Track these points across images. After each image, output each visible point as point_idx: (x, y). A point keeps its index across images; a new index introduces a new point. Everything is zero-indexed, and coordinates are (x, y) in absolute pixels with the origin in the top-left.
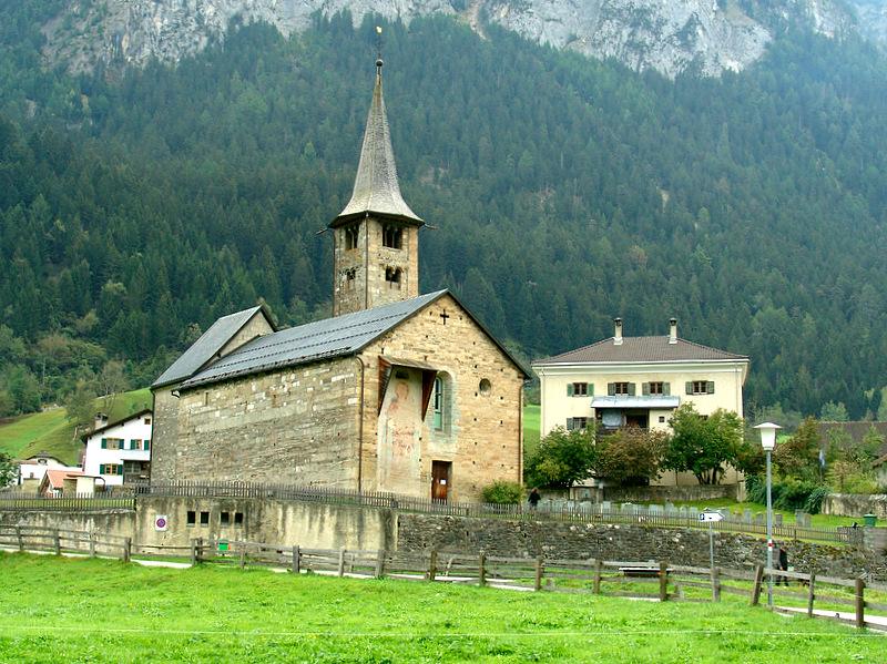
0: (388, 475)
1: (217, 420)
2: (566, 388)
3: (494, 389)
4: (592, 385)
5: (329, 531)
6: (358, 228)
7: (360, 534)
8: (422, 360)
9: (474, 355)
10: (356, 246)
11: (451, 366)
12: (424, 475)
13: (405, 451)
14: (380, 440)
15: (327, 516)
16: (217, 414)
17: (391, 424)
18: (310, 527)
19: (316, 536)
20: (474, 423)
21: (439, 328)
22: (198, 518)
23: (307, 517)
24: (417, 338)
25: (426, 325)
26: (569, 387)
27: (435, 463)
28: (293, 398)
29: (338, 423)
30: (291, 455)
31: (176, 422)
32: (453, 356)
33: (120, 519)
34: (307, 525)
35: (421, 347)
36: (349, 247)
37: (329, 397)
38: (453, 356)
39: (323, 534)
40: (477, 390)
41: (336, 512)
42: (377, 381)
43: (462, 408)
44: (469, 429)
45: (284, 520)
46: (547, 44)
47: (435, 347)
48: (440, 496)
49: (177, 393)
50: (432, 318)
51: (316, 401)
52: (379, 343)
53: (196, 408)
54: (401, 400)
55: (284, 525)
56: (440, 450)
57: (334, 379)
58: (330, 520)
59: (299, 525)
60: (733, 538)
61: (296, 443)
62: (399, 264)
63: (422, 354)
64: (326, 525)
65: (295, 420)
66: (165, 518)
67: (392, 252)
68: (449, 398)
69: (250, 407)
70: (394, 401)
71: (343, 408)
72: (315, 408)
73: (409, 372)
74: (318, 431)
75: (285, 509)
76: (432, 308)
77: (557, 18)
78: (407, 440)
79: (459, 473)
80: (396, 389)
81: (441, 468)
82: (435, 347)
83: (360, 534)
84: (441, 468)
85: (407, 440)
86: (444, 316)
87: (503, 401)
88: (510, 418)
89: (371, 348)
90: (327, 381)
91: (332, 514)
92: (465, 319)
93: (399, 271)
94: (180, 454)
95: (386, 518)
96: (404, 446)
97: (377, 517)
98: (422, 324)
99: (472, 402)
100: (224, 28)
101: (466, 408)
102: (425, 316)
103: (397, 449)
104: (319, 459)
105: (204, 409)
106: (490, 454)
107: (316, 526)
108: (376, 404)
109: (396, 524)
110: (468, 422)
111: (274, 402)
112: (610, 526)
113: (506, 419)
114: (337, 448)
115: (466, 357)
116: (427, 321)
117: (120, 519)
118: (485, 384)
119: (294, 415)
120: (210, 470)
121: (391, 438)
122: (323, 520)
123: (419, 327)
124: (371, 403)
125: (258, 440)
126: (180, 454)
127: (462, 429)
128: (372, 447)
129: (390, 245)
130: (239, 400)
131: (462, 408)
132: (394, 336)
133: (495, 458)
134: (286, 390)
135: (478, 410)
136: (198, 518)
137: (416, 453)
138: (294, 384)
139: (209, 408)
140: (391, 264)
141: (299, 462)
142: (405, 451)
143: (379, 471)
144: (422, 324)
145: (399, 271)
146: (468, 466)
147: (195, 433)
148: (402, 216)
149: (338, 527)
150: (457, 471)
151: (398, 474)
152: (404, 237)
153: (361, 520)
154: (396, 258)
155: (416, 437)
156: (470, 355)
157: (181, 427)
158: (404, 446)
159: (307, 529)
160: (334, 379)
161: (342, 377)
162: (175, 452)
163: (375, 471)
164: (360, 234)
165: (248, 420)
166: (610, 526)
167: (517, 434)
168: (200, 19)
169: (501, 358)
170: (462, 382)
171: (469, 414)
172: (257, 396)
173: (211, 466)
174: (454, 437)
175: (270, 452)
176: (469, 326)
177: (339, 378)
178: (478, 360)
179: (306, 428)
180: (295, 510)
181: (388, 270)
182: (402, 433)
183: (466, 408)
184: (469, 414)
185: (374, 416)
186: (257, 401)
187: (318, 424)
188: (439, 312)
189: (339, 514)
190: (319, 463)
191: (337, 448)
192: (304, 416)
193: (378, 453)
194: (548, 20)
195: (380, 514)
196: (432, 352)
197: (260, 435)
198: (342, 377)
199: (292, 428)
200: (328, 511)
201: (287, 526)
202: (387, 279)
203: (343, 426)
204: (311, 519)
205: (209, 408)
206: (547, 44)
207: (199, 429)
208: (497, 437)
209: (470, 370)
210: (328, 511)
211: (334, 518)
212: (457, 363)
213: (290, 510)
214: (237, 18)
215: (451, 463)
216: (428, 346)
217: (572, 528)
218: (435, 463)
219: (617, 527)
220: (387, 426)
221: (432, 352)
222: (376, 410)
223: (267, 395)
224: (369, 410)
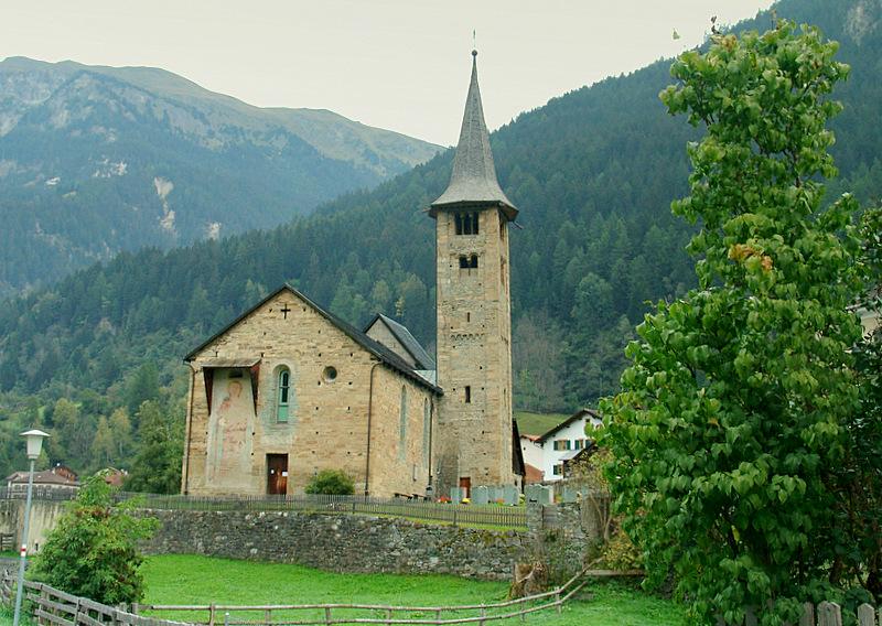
9: (318, 344)
11: (290, 358)
12: (256, 469)
13: (236, 447)
14: (210, 439)
17: (222, 422)
20: (315, 412)
23: (43, 514)
25: (264, 322)
27: (270, 456)
32: (293, 348)
38: (293, 348)
43: (302, 398)
47: (273, 343)
48: (275, 487)
50: (272, 314)
52: (214, 347)
54: (234, 399)
56: (275, 444)
60: (389, 524)
62: (473, 250)
67: (466, 239)
70: (227, 400)
73: (244, 371)
76: (272, 305)
78: (237, 436)
79: (295, 464)
80: (229, 388)
81: (277, 461)
84: (277, 461)
85: (237, 436)
86: (285, 311)
87: (351, 387)
88: (360, 402)
89: (203, 354)
92: (308, 310)
93: (475, 258)
96: (235, 442)
98: (260, 323)
99: (314, 391)
102: (264, 313)
103: (228, 445)
106: (333, 442)
108: (206, 405)
112: (280, 513)
113: (354, 404)
115: (309, 347)
121: (221, 435)
123: (256, 325)
127: (301, 419)
128: (202, 445)
131: (302, 398)
132: (229, 338)
133: (338, 446)
137: (249, 446)
140: (463, 252)
143: (208, 468)
144: (260, 323)
151: (227, 469)
152: (481, 220)
154: (469, 245)
155: (249, 433)
156: (314, 345)
158: (235, 442)
163: (203, 468)
166: (280, 513)
167: (367, 418)
169: (351, 342)
170: (305, 373)
171: (309, 404)
174: (292, 429)
176: (314, 315)
178: (322, 349)
183: (307, 398)
184: (309, 404)
185: (206, 416)
188: (280, 308)
193: (208, 450)
200: (57, 507)
209: (312, 360)
210: (57, 507)
216: (265, 343)
217: (247, 517)
218: (270, 456)
220: (217, 425)
222: (206, 410)
224: (200, 411)
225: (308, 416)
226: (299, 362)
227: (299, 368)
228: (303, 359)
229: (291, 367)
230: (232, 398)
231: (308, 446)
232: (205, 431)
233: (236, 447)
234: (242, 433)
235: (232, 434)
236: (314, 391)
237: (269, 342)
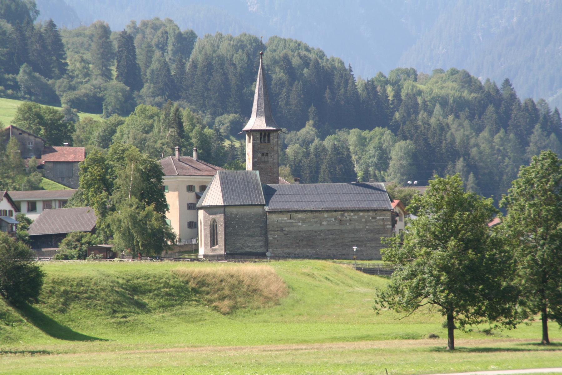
1: (300, 226)
16: (300, 224)
51: (369, 224)
53: (282, 220)
69: (325, 223)
72: (367, 227)
74: (370, 236)
105: (290, 221)
125: (330, 236)
134: (348, 218)
139: (293, 221)
147: (282, 230)
160: (378, 218)
161: (383, 217)
165: (322, 228)
172: (328, 219)
173: (297, 245)
179: (362, 234)
197: (333, 235)
198: (383, 217)
199: (353, 233)
223: (335, 219)
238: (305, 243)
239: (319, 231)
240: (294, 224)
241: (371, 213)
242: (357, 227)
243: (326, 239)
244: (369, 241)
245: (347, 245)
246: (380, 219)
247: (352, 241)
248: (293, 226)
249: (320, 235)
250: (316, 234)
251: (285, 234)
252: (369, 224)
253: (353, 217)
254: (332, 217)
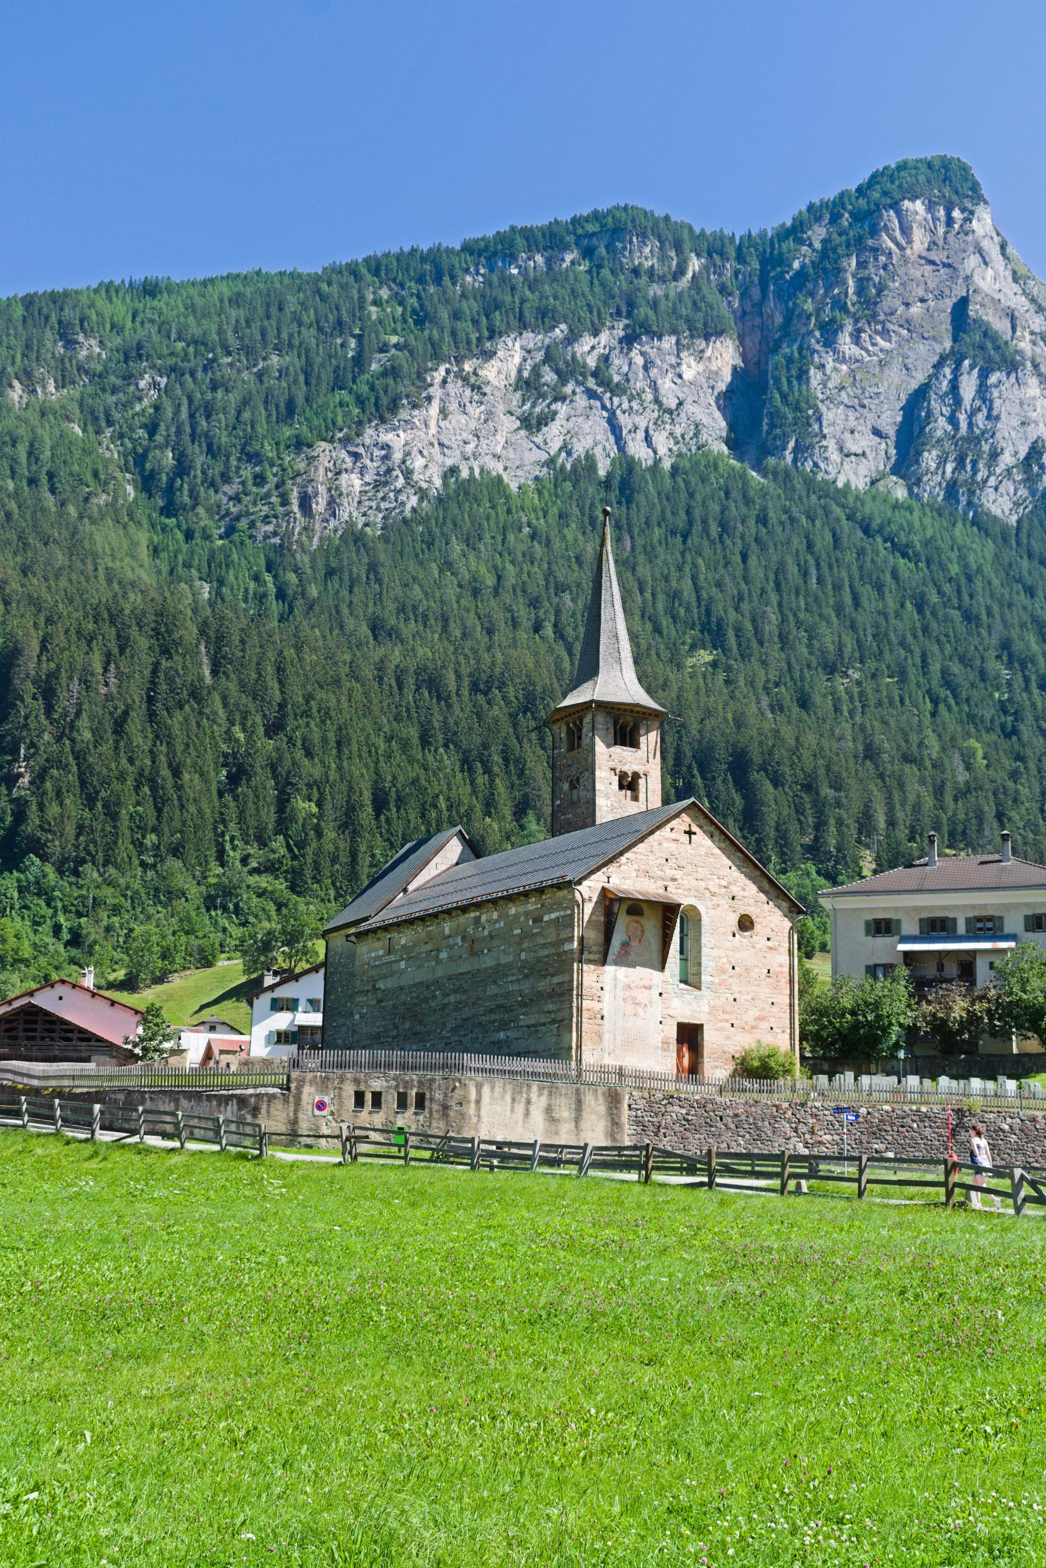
0: (618, 1042)
1: (403, 972)
2: (863, 926)
3: (758, 927)
4: (898, 921)
5: (538, 1115)
6: (581, 722)
7: (577, 1120)
8: (662, 891)
10: (579, 746)
12: (665, 1042)
14: (607, 996)
15: (534, 1096)
16: (403, 964)
18: (512, 1111)
19: (520, 1123)
21: (683, 849)
22: (368, 1098)
23: (508, 1098)
24: (654, 862)
25: (666, 845)
26: (868, 924)
28: (495, 943)
29: (552, 975)
30: (493, 1017)
31: (352, 975)
33: (269, 1101)
34: (508, 1108)
35: (660, 873)
36: (571, 748)
37: (541, 941)
38: (702, 884)
39: (531, 1120)
40: (735, 928)
41: (546, 1092)
42: (602, 919)
44: (724, 980)
45: (478, 1102)
46: (847, 485)
47: (678, 874)
49: (353, 938)
50: (673, 835)
51: (525, 945)
53: (377, 958)
55: (478, 1109)
57: (546, 918)
58: (539, 1102)
59: (498, 1109)
61: (501, 1001)
63: (661, 883)
64: (531, 1108)
65: (498, 973)
66: (326, 1099)
68: (698, 940)
69: (443, 955)
71: (559, 955)
72: (523, 956)
73: (644, 906)
74: (526, 986)
75: (479, 1087)
77: (859, 451)
78: (642, 996)
82: (678, 874)
83: (577, 1120)
86: (690, 833)
87: (770, 944)
90: (538, 920)
91: (540, 1095)
94: (357, 1017)
95: (613, 1099)
97: (601, 1100)
98: (660, 844)
99: (728, 944)
100: (438, 482)
101: (722, 953)
102: (665, 832)
103: (629, 1008)
104: (529, 1023)
105: (387, 959)
106: (754, 1013)
107: (520, 1108)
108: (601, 949)
109: (626, 1107)
110: (724, 972)
111: (472, 947)
112: (914, 1108)
114: (551, 1007)
115: (720, 886)
116: (667, 839)
117: (269, 1101)
118: (746, 924)
119: (498, 964)
120: (395, 1037)
121: (620, 993)
122: (528, 1102)
123: (656, 847)
124: (594, 948)
125: (452, 998)
126: (357, 1017)
127: (716, 980)
129: (624, 744)
130: (429, 947)
131: (715, 952)
133: (760, 1019)
134: (486, 933)
135: (737, 955)
136: (368, 1098)
138: (497, 926)
139: (392, 958)
140: (625, 768)
141: (503, 1026)
142: (640, 1011)
143: (606, 1037)
145: (636, 776)
146: (722, 1029)
147: (376, 990)
148: (638, 705)
149: (549, 1110)
150: (710, 1037)
153: (579, 1102)
154: (629, 759)
157: (358, 982)
159: (508, 1113)
160: (546, 918)
162: (352, 1015)
164: (584, 730)
165: (440, 973)
168: (408, 474)
172: (451, 941)
173: (395, 1033)
175: (466, 1013)
177: (553, 916)
178: (735, 890)
179: (512, 982)
180: (493, 1088)
181: (623, 776)
182: (636, 987)
183: (722, 953)
184: (725, 960)
186: (451, 947)
187: (526, 976)
189: (550, 1094)
190: (528, 1027)
191: (551, 1007)
192: (509, 966)
193: (605, 1013)
194: (847, 456)
195: (604, 1094)
196: (674, 880)
197: (455, 992)
199: (494, 982)
200: (535, 1088)
201: (483, 1112)
202: (621, 787)
203: (556, 980)
204: (513, 1100)
205: (392, 958)
206: (847, 485)
207: (381, 985)
208: (765, 992)
209: (725, 903)
210: (535, 1088)
211: (544, 1099)
212: (708, 895)
213: (486, 1090)
214: (453, 470)
215: (702, 1026)
216: (670, 873)
219: (924, 1109)
221: (674, 880)
223: (464, 938)
225: (724, 977)
226: (710, 904)
227: (711, 912)
228: (715, 901)
229: (701, 909)
230: (633, 944)
231: (727, 1016)
232: (599, 985)
233: (640, 1011)
234: (646, 992)
235: (635, 993)
236: (728, 944)
237: (674, 872)
238: (407, 1025)
239: (433, 983)
240: (395, 967)
241: (532, 905)
242: (503, 961)
243: (445, 1007)
244: (525, 1005)
245: (480, 1024)
246: (551, 921)
247: (491, 1011)
248: (392, 974)
249: (435, 997)
250: (427, 994)
251: (379, 1001)
252: (525, 945)
253: (497, 926)
254: (457, 934)
